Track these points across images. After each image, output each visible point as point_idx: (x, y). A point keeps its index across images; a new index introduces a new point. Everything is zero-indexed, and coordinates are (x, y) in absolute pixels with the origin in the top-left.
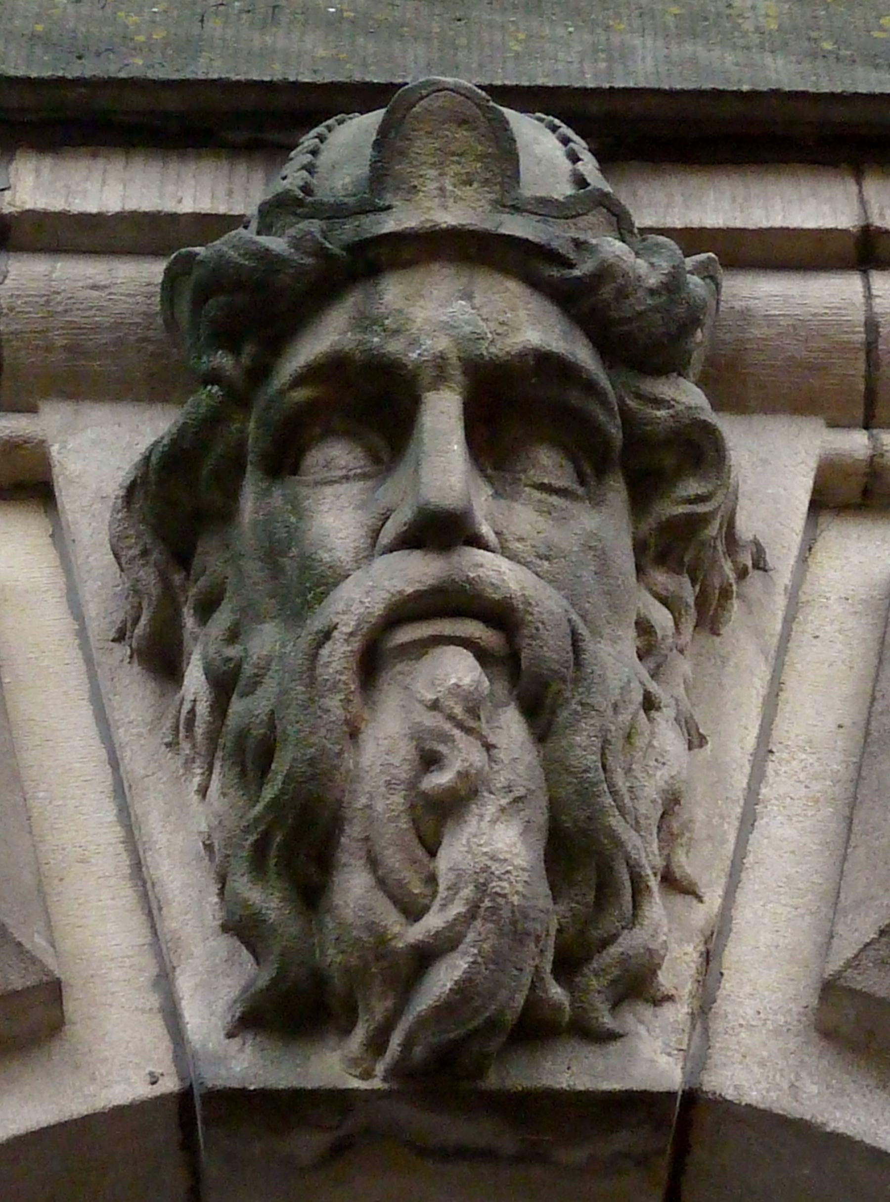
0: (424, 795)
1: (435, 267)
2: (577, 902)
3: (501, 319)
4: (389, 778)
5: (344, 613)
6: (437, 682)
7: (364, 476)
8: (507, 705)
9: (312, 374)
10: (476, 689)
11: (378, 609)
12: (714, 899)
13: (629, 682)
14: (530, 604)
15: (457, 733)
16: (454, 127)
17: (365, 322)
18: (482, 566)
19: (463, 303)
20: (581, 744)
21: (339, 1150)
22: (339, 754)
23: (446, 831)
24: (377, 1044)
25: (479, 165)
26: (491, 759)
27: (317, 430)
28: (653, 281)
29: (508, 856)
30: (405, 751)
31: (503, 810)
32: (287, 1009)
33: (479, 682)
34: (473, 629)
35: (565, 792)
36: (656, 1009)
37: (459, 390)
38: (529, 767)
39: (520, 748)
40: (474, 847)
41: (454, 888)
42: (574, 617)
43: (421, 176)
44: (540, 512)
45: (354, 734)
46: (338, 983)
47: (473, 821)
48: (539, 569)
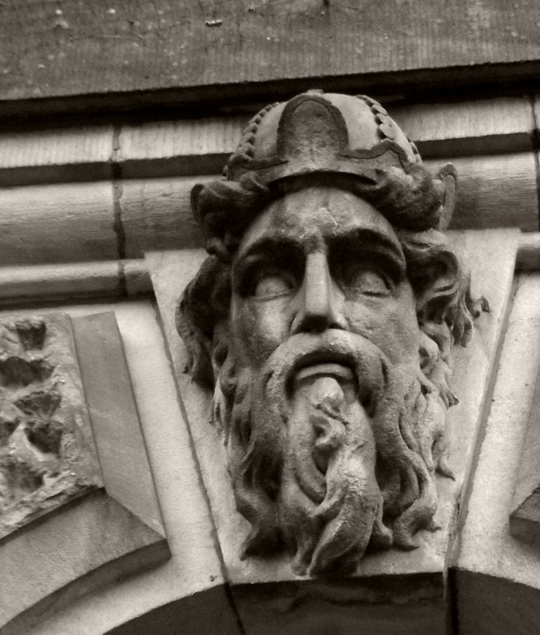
0: (317, 448)
1: (310, 190)
2: (392, 490)
3: (342, 214)
4: (301, 441)
5: (276, 365)
6: (319, 396)
7: (285, 295)
8: (354, 402)
9: (255, 249)
10: (337, 398)
11: (291, 363)
12: (461, 479)
13: (413, 383)
14: (361, 355)
15: (329, 419)
16: (315, 118)
17: (278, 222)
18: (337, 339)
19: (323, 209)
20: (389, 418)
21: (296, 605)
22: (279, 431)
23: (329, 463)
24: (307, 559)
25: (328, 136)
26: (347, 429)
27: (262, 274)
28: (415, 187)
29: (356, 474)
30: (308, 428)
31: (353, 452)
32: (265, 546)
33: (338, 395)
34: (336, 369)
35: (384, 440)
36: (434, 534)
37: (323, 252)
38: (366, 431)
39: (361, 423)
40: (341, 471)
41: (333, 490)
42: (384, 357)
43: (301, 145)
44: (367, 306)
45: (285, 420)
46: (287, 534)
47: (340, 459)
48: (367, 335)
